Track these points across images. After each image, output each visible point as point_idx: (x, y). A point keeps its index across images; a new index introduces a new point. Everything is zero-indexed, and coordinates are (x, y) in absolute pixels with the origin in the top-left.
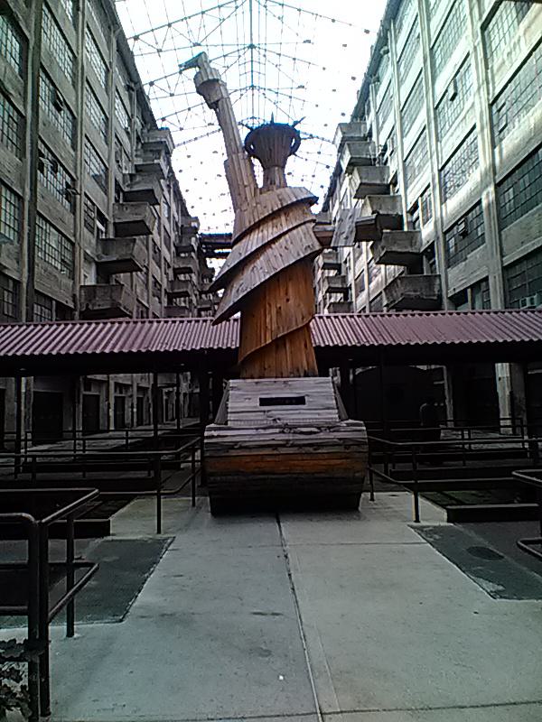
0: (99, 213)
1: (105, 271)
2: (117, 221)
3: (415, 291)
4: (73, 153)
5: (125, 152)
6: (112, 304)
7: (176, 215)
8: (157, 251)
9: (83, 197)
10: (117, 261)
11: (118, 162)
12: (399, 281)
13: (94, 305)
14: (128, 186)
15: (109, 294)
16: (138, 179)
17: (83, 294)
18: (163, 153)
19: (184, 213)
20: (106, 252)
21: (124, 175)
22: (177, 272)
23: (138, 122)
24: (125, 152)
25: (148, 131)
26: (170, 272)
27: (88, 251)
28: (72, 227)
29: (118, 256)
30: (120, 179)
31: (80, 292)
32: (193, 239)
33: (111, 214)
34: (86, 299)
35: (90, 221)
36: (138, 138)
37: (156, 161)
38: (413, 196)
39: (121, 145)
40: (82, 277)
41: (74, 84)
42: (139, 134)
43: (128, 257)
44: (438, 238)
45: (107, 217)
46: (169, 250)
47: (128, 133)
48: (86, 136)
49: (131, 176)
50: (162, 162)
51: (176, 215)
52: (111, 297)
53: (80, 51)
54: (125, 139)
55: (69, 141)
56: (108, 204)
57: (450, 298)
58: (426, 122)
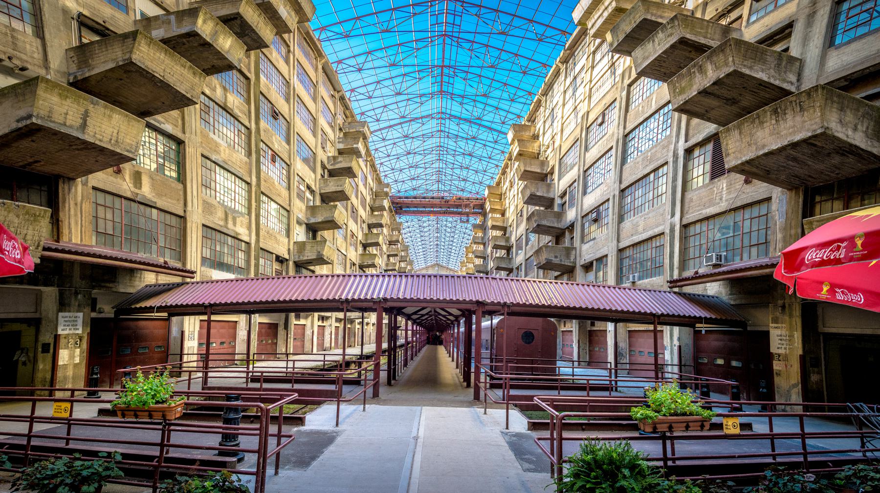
0: (309, 187)
1: (313, 230)
2: (323, 191)
3: (556, 257)
6: (317, 255)
8: (354, 211)
9: (297, 178)
12: (544, 249)
22: (370, 226)
26: (365, 226)
33: (318, 186)
43: (330, 219)
45: (314, 188)
57: (582, 266)
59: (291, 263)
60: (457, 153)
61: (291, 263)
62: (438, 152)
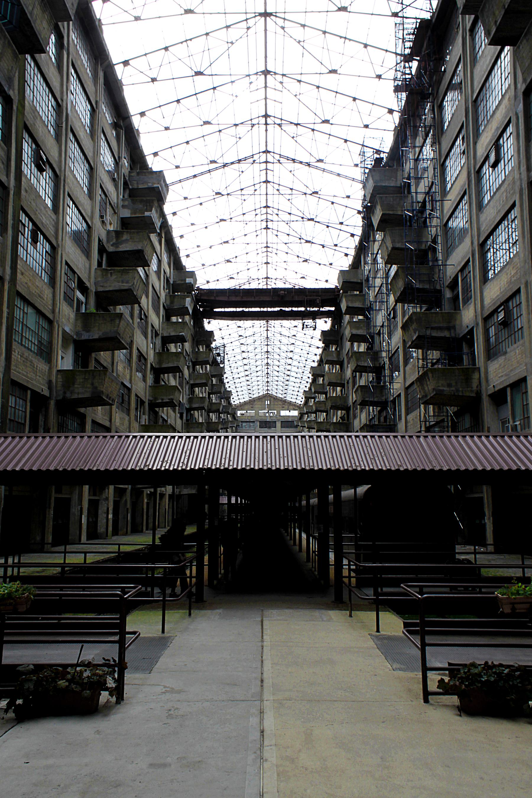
2: (100, 289)
4: (54, 216)
5: (110, 204)
7: (168, 270)
8: (144, 317)
10: (99, 340)
11: (102, 217)
13: (72, 393)
14: (112, 245)
15: (90, 381)
16: (125, 237)
17: (60, 380)
18: (156, 204)
19: (177, 264)
20: (86, 327)
21: (109, 232)
22: (166, 340)
23: (125, 162)
24: (110, 204)
25: (138, 174)
26: (158, 341)
27: (67, 329)
28: (50, 302)
29: (101, 333)
30: (104, 237)
31: (57, 378)
32: (188, 300)
33: (92, 280)
34: (63, 386)
35: (70, 294)
36: (125, 184)
37: (147, 214)
38: (451, 271)
39: (106, 196)
40: (60, 358)
41: (58, 137)
42: (127, 178)
44: (477, 324)
45: (88, 284)
46: (158, 315)
47: (114, 180)
48: (69, 195)
49: (118, 234)
50: (154, 214)
51: (168, 270)
52: (92, 384)
53: (65, 97)
54: (110, 187)
55: (49, 203)
56: (90, 268)
58: (467, 186)
59: (52, 403)
60: (293, 218)
61: (52, 403)
62: (264, 217)
